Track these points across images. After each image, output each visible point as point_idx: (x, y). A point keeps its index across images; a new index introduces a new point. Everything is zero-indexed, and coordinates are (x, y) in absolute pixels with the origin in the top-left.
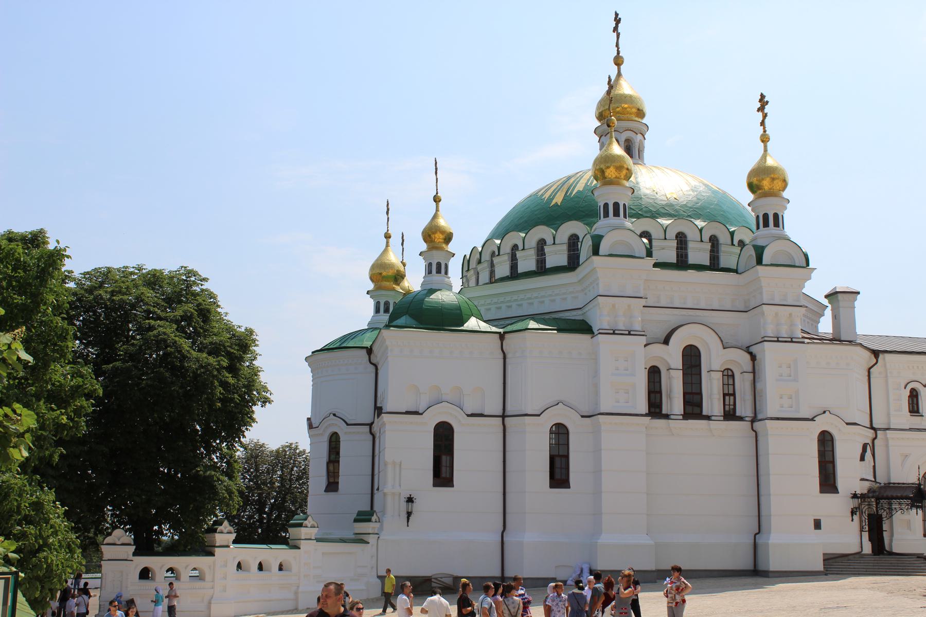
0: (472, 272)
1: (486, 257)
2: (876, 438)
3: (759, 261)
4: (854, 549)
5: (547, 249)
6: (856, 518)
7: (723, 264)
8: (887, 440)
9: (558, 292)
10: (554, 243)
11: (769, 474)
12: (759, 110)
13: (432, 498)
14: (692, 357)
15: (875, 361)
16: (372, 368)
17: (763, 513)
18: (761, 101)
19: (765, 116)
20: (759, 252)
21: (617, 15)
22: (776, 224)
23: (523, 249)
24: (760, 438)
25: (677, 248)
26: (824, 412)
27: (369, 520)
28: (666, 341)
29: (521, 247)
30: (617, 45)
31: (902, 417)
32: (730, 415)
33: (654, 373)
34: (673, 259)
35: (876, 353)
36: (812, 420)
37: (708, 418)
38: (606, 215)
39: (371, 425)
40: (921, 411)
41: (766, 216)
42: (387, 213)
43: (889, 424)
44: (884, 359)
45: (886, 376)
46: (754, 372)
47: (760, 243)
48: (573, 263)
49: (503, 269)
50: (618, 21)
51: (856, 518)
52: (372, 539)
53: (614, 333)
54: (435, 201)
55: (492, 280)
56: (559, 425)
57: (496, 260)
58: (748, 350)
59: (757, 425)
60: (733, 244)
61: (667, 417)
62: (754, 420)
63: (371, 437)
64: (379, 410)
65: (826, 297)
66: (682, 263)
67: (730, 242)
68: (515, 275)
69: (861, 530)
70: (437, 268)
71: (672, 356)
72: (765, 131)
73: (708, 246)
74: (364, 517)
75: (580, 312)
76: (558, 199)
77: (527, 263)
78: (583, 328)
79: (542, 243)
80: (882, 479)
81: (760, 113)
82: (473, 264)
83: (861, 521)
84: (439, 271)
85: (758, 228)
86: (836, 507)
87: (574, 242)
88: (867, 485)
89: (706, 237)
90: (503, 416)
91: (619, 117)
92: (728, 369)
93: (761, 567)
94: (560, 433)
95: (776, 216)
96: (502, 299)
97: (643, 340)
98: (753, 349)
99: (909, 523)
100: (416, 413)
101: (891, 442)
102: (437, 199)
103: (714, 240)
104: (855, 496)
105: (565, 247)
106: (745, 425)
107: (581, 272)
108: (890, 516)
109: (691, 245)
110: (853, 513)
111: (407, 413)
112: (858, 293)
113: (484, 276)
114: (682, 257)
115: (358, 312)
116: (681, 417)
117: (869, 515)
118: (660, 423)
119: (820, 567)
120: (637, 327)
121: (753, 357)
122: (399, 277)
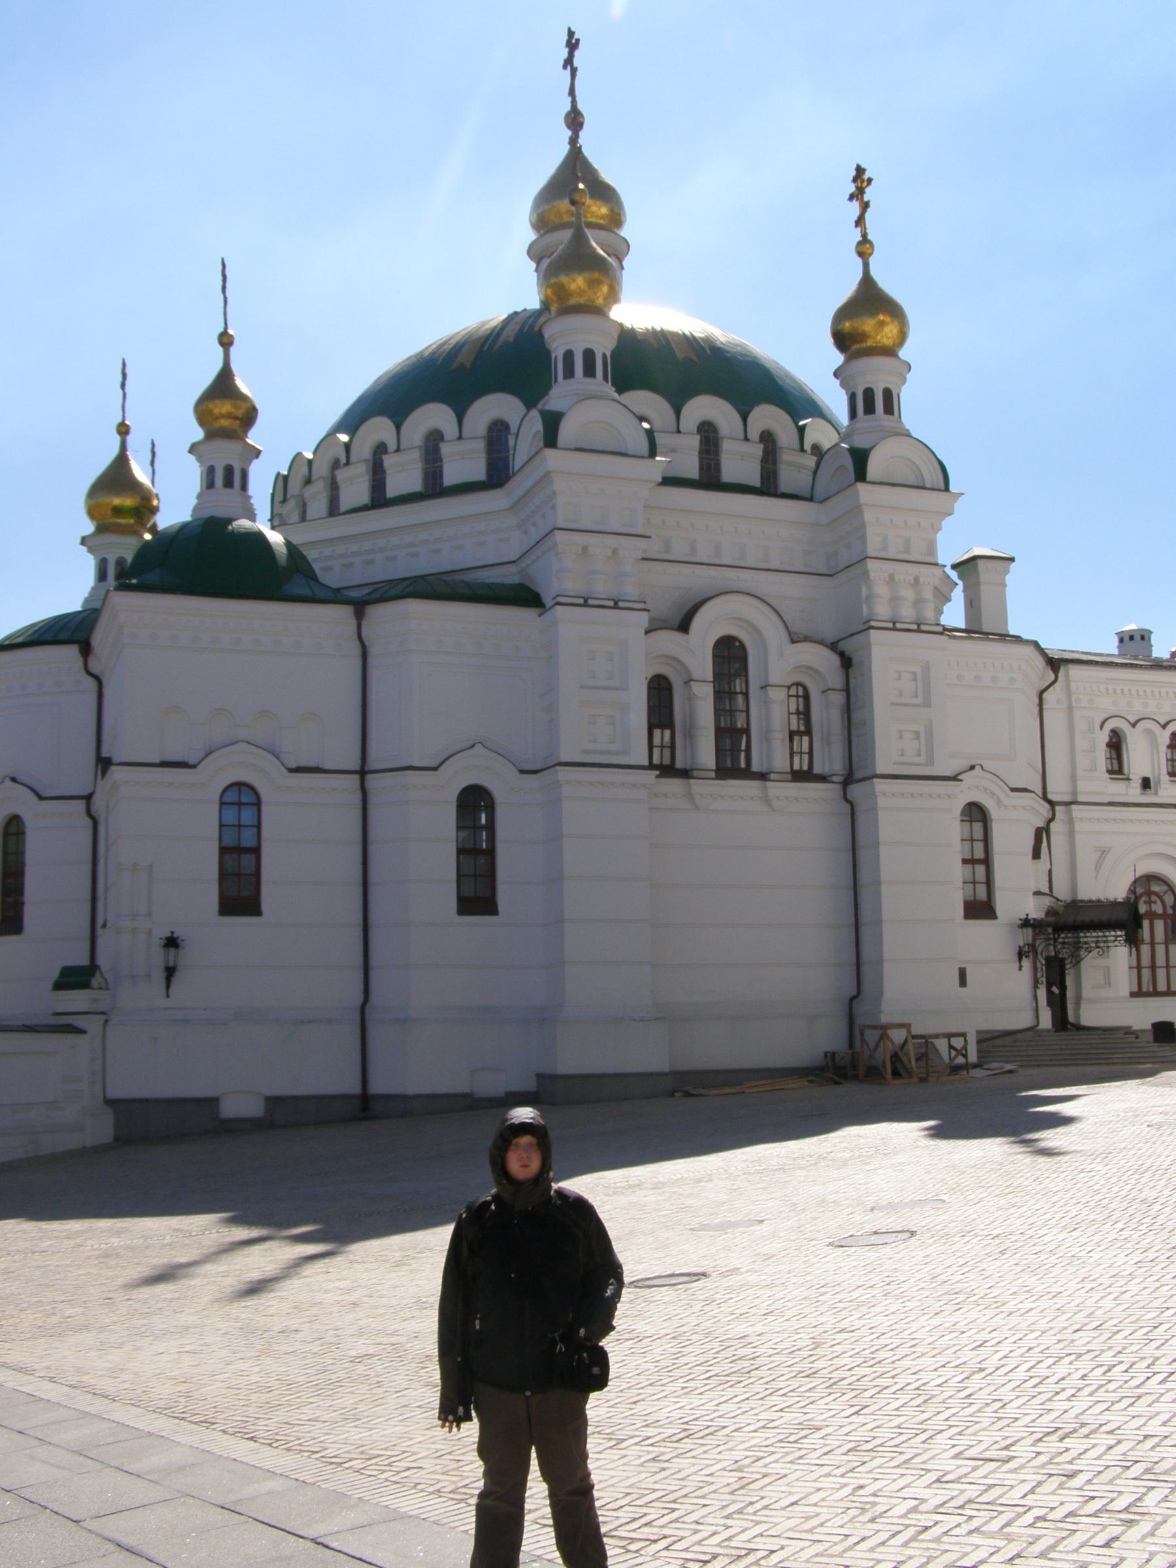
0: (292, 503)
1: (321, 470)
2: (1052, 819)
3: (861, 474)
4: (1023, 1020)
5: (445, 449)
6: (1026, 963)
7: (783, 487)
8: (1070, 821)
9: (470, 533)
10: (460, 438)
11: (878, 883)
12: (851, 197)
14: (730, 655)
15: (1052, 677)
16: (91, 684)
17: (867, 954)
18: (855, 180)
19: (865, 206)
20: (860, 458)
21: (571, 34)
22: (889, 409)
23: (398, 450)
25: (701, 452)
26: (972, 768)
27: (86, 985)
28: (684, 626)
29: (392, 446)
30: (572, 92)
31: (1097, 783)
33: (660, 692)
34: (693, 472)
35: (1055, 664)
36: (955, 778)
37: (763, 776)
38: (569, 373)
39: (88, 798)
40: (1126, 771)
41: (869, 394)
42: (123, 386)
43: (1074, 792)
44: (1067, 675)
45: (1070, 708)
46: (847, 690)
47: (860, 442)
48: (498, 473)
49: (356, 490)
50: (572, 44)
51: (1026, 963)
52: (92, 1025)
53: (585, 605)
54: (222, 344)
55: (333, 510)
57: (341, 475)
58: (833, 646)
59: (855, 790)
60: (802, 450)
61: (685, 774)
62: (848, 780)
63: (89, 822)
64: (104, 764)
65: (954, 567)
66: (710, 479)
67: (796, 445)
68: (379, 500)
69: (1036, 986)
70: (227, 478)
72: (864, 235)
73: (758, 450)
74: (74, 978)
75: (513, 569)
76: (465, 359)
77: (404, 475)
78: (526, 597)
79: (434, 440)
80: (1062, 891)
81: (855, 206)
82: (294, 487)
83: (1035, 970)
84: (228, 483)
85: (853, 414)
86: (990, 944)
87: (498, 434)
89: (754, 432)
90: (363, 773)
91: (577, 222)
92: (797, 684)
95: (888, 395)
96: (354, 547)
98: (845, 646)
99: (1107, 971)
101: (1078, 826)
102: (226, 341)
103: (767, 438)
104: (1026, 923)
105: (481, 445)
107: (516, 487)
108: (1077, 962)
110: (1021, 955)
111: (164, 764)
112: (1012, 560)
113: (317, 507)
114: (709, 467)
115: (65, 582)
116: (713, 774)
117: (1048, 959)
118: (674, 785)
120: (630, 590)
121: (846, 662)
122: (145, 507)
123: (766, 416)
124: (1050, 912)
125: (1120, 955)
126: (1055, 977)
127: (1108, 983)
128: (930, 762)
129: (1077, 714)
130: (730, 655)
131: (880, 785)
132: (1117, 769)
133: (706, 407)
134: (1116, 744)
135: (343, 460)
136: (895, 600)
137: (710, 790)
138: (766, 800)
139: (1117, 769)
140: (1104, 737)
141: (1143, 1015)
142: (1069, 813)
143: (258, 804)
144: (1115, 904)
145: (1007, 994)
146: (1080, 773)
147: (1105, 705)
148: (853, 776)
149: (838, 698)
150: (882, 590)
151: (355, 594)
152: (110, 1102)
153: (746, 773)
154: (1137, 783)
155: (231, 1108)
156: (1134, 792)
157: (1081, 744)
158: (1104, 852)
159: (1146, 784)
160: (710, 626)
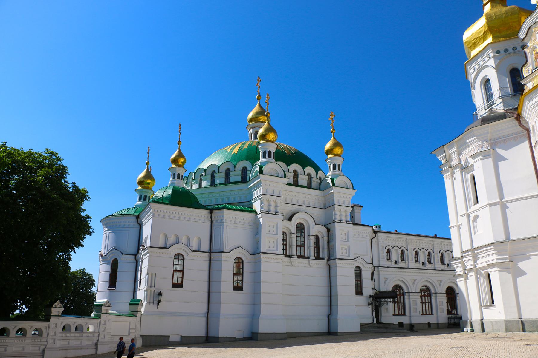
5: (231, 173)
6: (370, 306)
8: (379, 271)
11: (337, 286)
13: (170, 294)
14: (300, 228)
24: (332, 269)
28: (290, 219)
32: (318, 257)
37: (308, 258)
43: (379, 264)
45: (378, 243)
48: (244, 180)
50: (259, 80)
51: (370, 306)
56: (238, 258)
58: (325, 226)
59: (331, 262)
61: (290, 256)
66: (295, 184)
71: (292, 226)
87: (244, 171)
88: (375, 291)
89: (306, 174)
90: (210, 252)
93: (332, 330)
94: (239, 262)
97: (282, 217)
98: (329, 226)
100: (165, 248)
101: (380, 273)
103: (309, 175)
104: (370, 296)
105: (240, 172)
106: (324, 262)
108: (381, 307)
109: (300, 176)
110: (369, 305)
118: (288, 259)
119: (359, 330)
121: (328, 230)
123: (309, 170)
124: (376, 294)
125: (391, 305)
126: (377, 311)
127: (388, 312)
128: (349, 256)
129: (380, 245)
130: (300, 228)
131: (337, 261)
132: (389, 259)
133: (295, 167)
134: (389, 251)
135: (204, 174)
136: (341, 215)
137: (295, 260)
138: (309, 264)
139: (389, 259)
140: (386, 251)
141: (396, 320)
142: (378, 269)
143: (184, 259)
144: (389, 292)
145: (366, 315)
146: (381, 259)
147: (386, 243)
148: (330, 258)
149: (326, 239)
150: (337, 213)
151: (209, 207)
152: (140, 335)
153: (303, 257)
154: (394, 262)
155: (171, 339)
156: (393, 265)
157: (381, 252)
158: (386, 279)
159: (396, 262)
160: (296, 220)
